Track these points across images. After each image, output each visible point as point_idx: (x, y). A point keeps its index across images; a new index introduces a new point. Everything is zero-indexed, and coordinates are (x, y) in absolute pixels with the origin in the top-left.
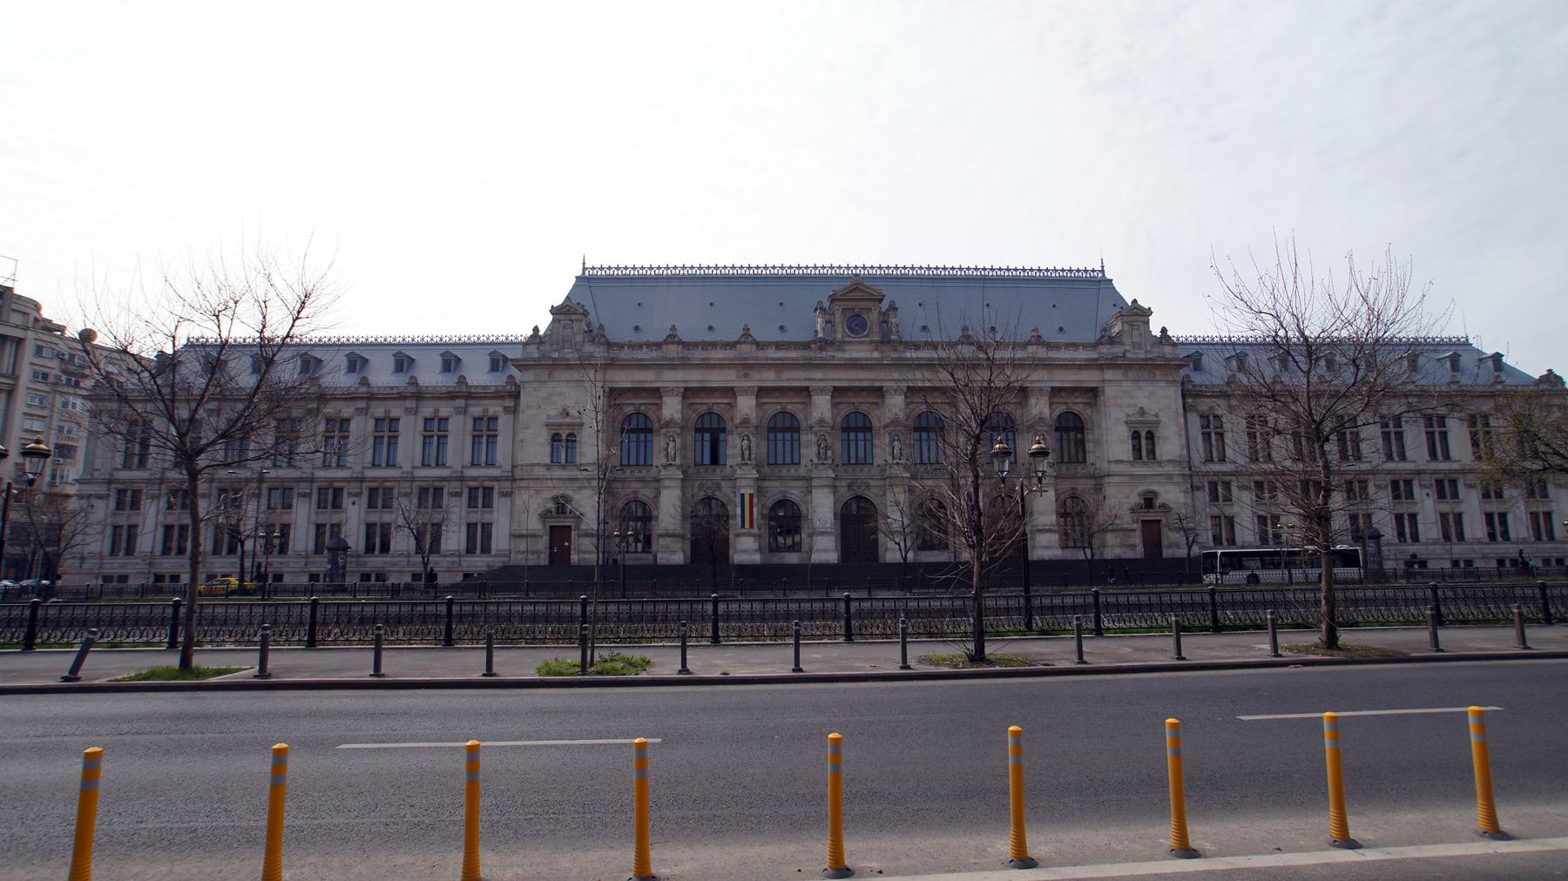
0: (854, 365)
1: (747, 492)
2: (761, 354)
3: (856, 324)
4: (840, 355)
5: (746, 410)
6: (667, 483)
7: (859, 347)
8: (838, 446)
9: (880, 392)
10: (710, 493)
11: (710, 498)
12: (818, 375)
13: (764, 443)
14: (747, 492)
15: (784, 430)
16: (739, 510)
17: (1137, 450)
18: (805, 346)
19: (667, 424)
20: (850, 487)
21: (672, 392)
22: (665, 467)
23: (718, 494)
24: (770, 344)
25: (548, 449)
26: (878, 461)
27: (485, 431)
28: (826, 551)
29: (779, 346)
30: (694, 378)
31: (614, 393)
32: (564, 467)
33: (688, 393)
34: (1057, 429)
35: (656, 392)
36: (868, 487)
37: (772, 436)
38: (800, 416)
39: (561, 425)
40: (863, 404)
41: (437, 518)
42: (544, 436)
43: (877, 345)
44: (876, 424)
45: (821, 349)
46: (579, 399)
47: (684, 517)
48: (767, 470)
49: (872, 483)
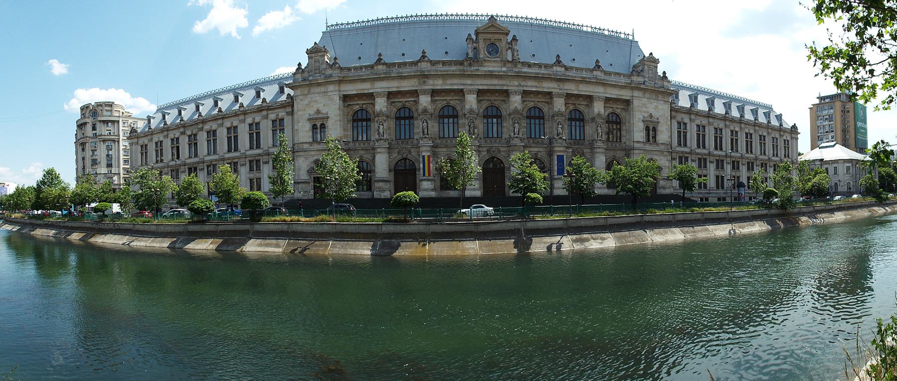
0: (491, 75)
1: (426, 154)
2: (434, 68)
3: (493, 49)
4: (482, 69)
5: (425, 104)
6: (379, 150)
7: (494, 64)
8: (481, 126)
9: (506, 93)
10: (405, 156)
11: (405, 159)
12: (469, 82)
13: (436, 125)
14: (426, 154)
15: (449, 117)
16: (421, 166)
17: (648, 135)
18: (461, 63)
19: (378, 115)
20: (488, 151)
21: (380, 95)
22: (377, 140)
23: (409, 157)
24: (439, 62)
25: (311, 134)
26: (505, 136)
27: (278, 126)
28: (474, 190)
29: (444, 63)
30: (394, 85)
31: (346, 98)
32: (319, 143)
33: (390, 95)
34: (607, 122)
35: (371, 96)
36: (499, 151)
37: (441, 120)
38: (458, 108)
39: (317, 119)
40: (496, 100)
41: (258, 175)
42: (308, 126)
43: (505, 62)
44: (504, 113)
45: (470, 65)
46: (328, 103)
47: (390, 171)
48: (438, 141)
49: (502, 149)
